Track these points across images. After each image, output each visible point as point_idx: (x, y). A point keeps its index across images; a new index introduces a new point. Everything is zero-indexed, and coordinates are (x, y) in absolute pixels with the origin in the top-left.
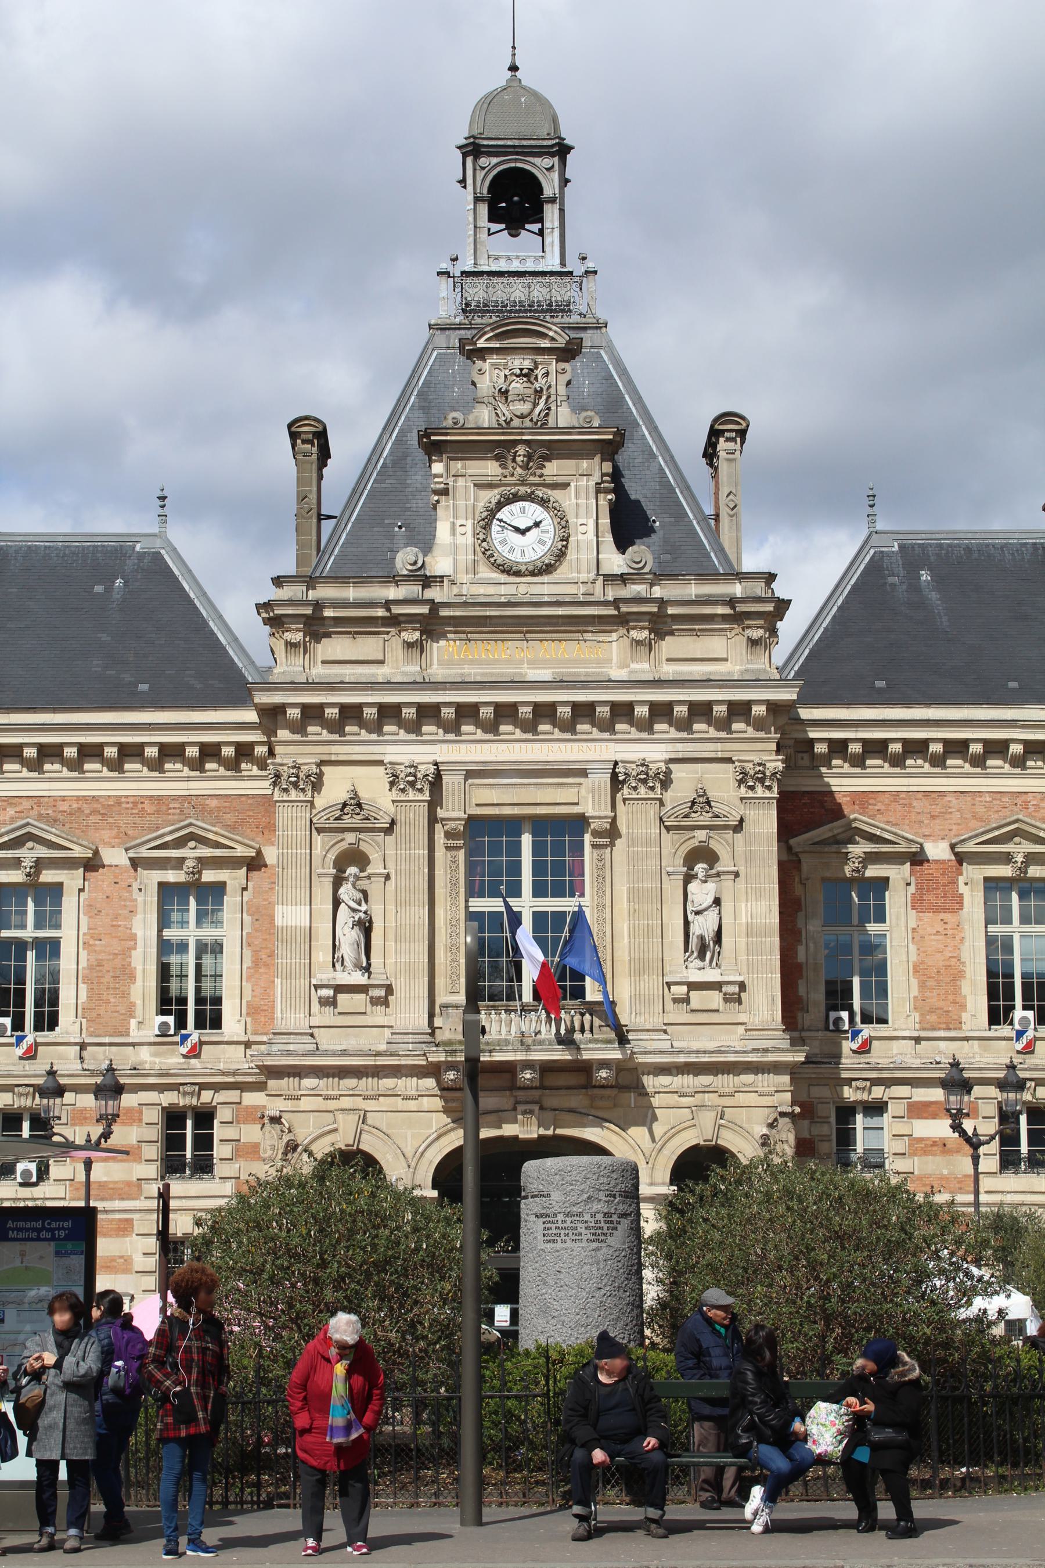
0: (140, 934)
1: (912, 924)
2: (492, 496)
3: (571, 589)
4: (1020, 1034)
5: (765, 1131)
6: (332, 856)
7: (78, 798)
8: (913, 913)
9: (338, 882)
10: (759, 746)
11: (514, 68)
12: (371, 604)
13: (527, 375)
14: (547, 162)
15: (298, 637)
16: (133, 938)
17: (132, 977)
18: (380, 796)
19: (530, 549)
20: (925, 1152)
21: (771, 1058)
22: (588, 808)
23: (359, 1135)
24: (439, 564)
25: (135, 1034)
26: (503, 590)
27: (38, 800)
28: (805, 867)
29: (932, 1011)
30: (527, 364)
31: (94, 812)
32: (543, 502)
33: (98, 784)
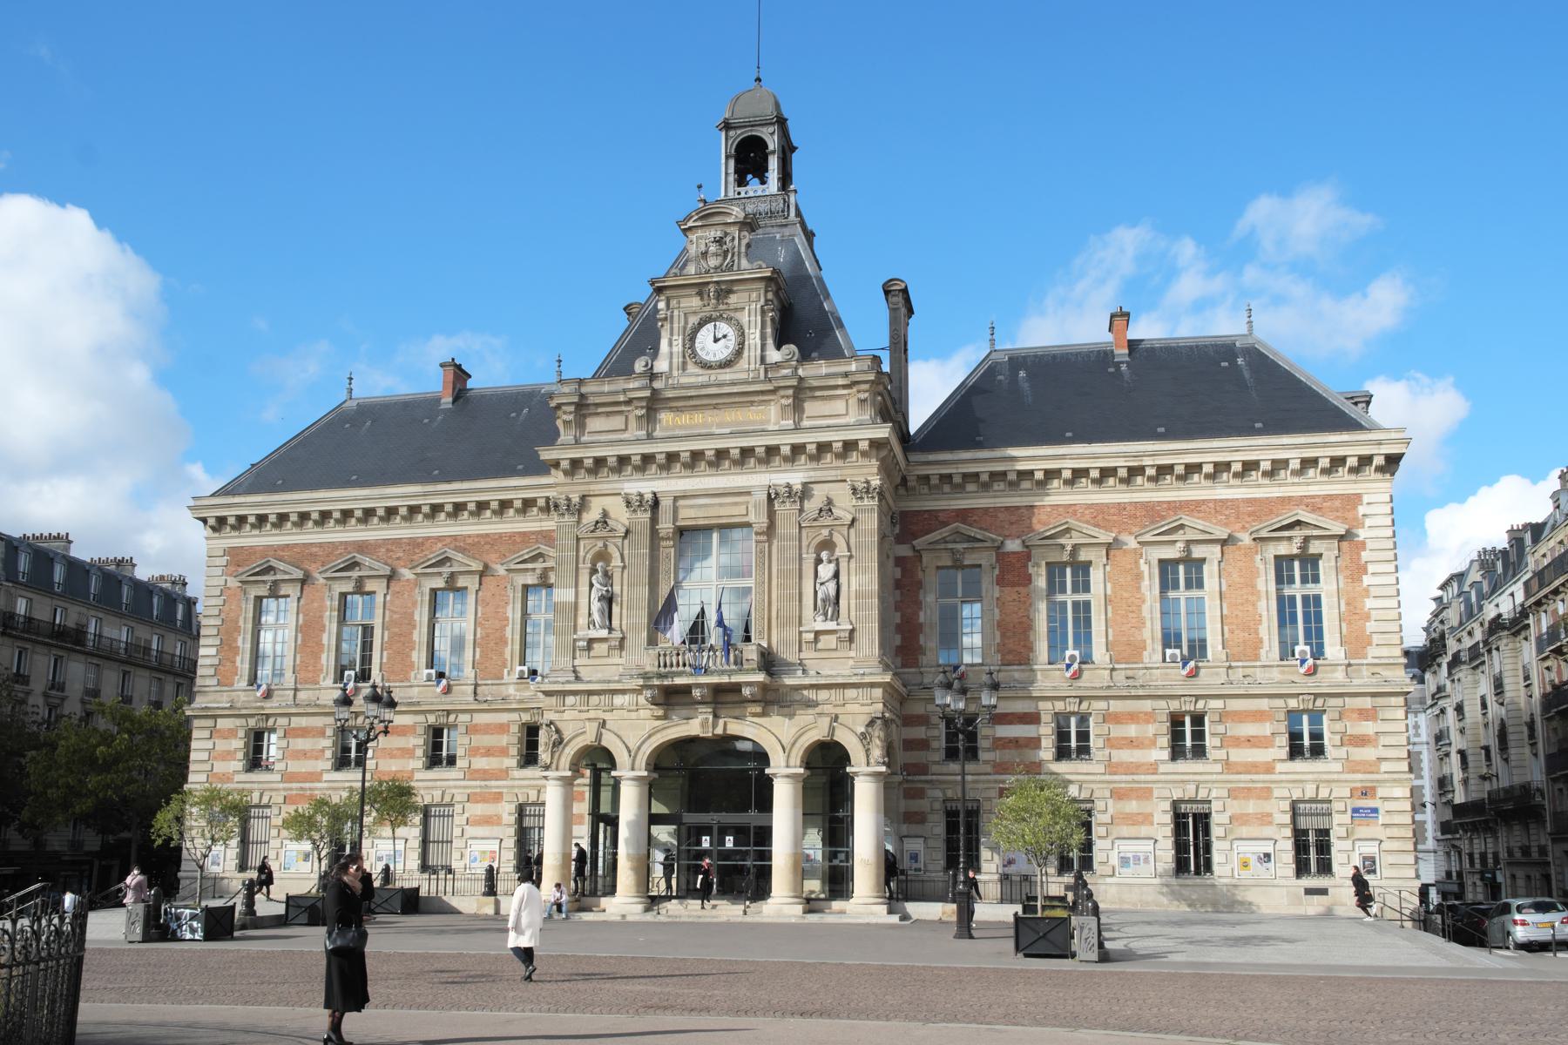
0: (510, 615)
1: (997, 595)
2: (693, 320)
3: (744, 376)
4: (1069, 666)
5: (863, 729)
6: (589, 556)
8: (997, 588)
9: (594, 571)
10: (865, 471)
12: (617, 393)
13: (719, 241)
14: (771, 129)
15: (571, 417)
17: (506, 643)
18: (621, 516)
19: (720, 352)
20: (1004, 747)
21: (867, 680)
22: (752, 518)
23: (599, 736)
24: (661, 365)
25: (506, 679)
26: (700, 379)
27: (455, 538)
28: (924, 560)
29: (1010, 652)
33: (489, 526)
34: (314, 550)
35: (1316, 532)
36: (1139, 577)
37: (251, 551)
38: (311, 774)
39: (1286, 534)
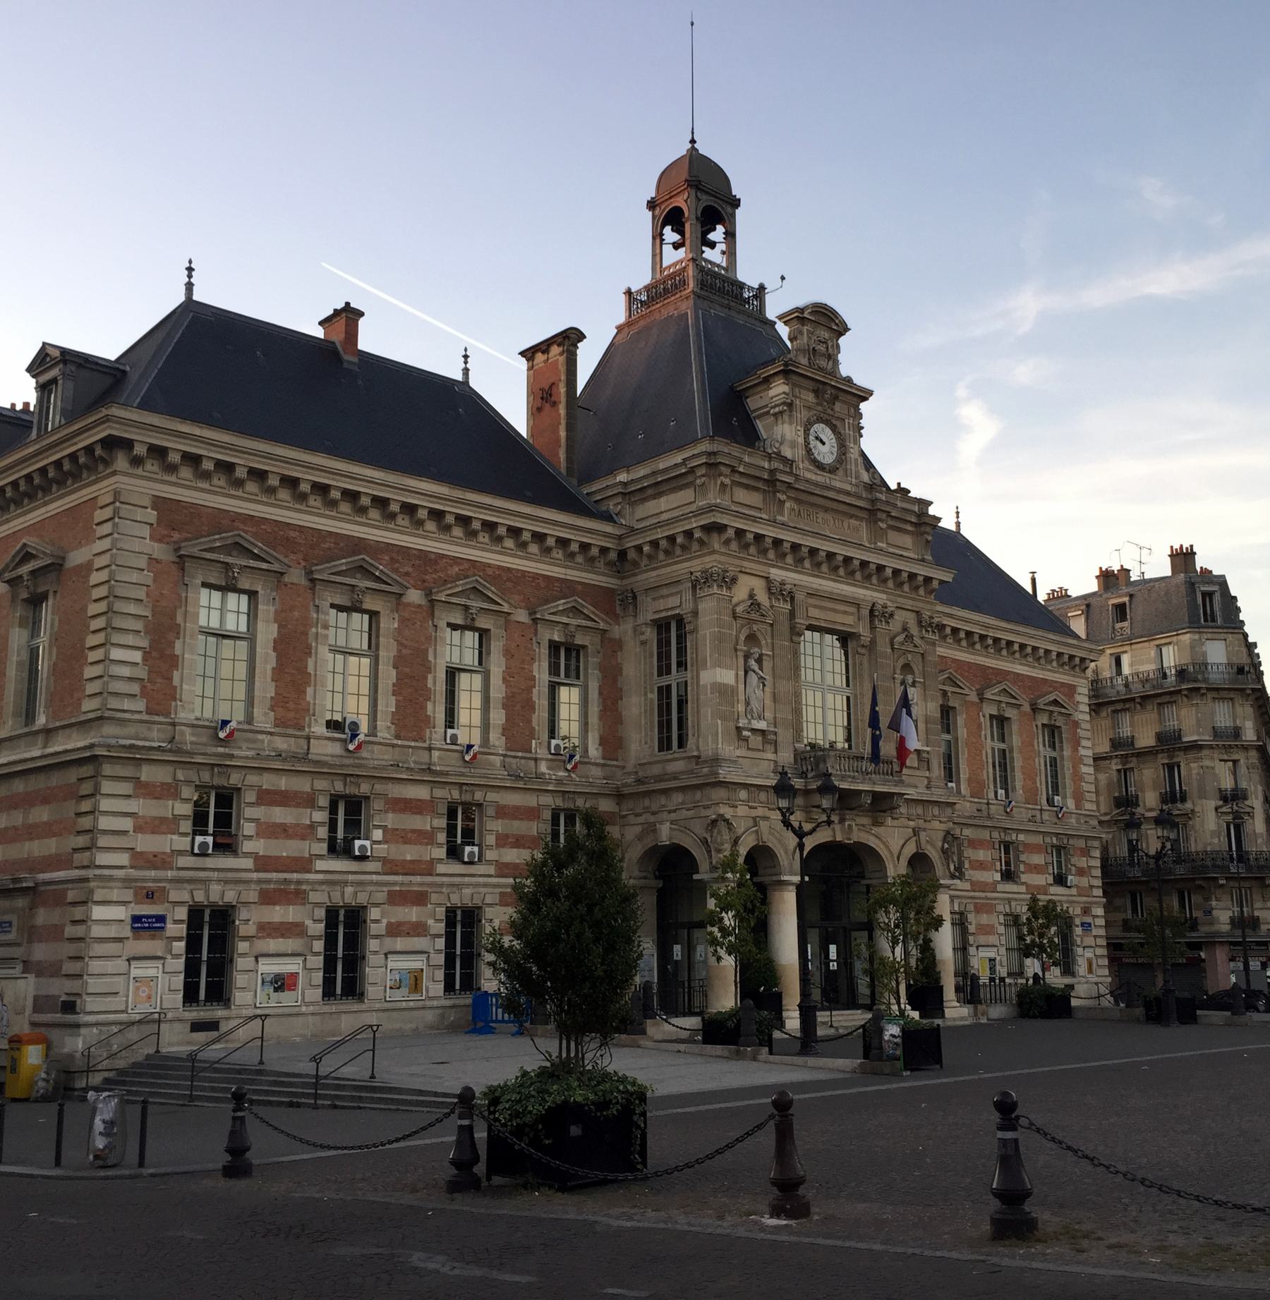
7: (499, 567)
9: (747, 657)
11: (693, 141)
16: (533, 678)
30: (827, 336)
31: (509, 580)
32: (834, 429)
34: (292, 534)
35: (1063, 710)
36: (980, 725)
37: (194, 511)
38: (296, 859)
39: (1051, 708)
